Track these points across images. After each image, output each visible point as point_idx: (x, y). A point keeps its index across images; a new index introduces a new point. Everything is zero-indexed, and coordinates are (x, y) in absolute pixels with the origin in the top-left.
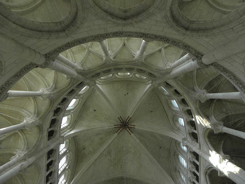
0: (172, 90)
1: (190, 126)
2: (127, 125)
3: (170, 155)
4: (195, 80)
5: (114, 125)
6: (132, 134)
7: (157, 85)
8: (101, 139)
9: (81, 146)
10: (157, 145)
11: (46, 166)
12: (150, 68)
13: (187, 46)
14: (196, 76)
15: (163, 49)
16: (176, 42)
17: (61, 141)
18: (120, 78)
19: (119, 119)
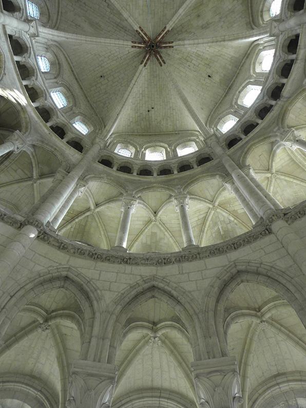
0: (69, 136)
1: (28, 65)
2: (147, 47)
4: (33, 160)
5: (173, 47)
6: (136, 28)
7: (97, 140)
8: (199, 16)
10: (85, 3)
12: (112, 178)
13: (62, 249)
14: (33, 167)
15: (92, 207)
16: (79, 254)
17: (275, 27)
18: (162, 142)
19: (163, 61)
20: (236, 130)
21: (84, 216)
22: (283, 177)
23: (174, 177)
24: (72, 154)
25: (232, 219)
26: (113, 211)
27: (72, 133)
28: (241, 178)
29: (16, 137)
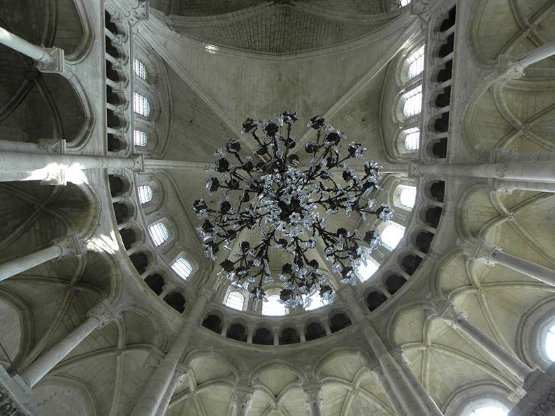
0: (169, 288)
3: (170, 106)
4: (120, 328)
7: (204, 290)
9: (370, 126)
10: (198, 126)
11: (455, 68)
12: (221, 351)
14: (118, 335)
17: (415, 169)
20: (377, 282)
21: (179, 400)
22: (441, 351)
23: (302, 347)
24: (170, 317)
25: (379, 407)
26: (220, 394)
27: (173, 282)
28: (393, 371)
29: (103, 309)
